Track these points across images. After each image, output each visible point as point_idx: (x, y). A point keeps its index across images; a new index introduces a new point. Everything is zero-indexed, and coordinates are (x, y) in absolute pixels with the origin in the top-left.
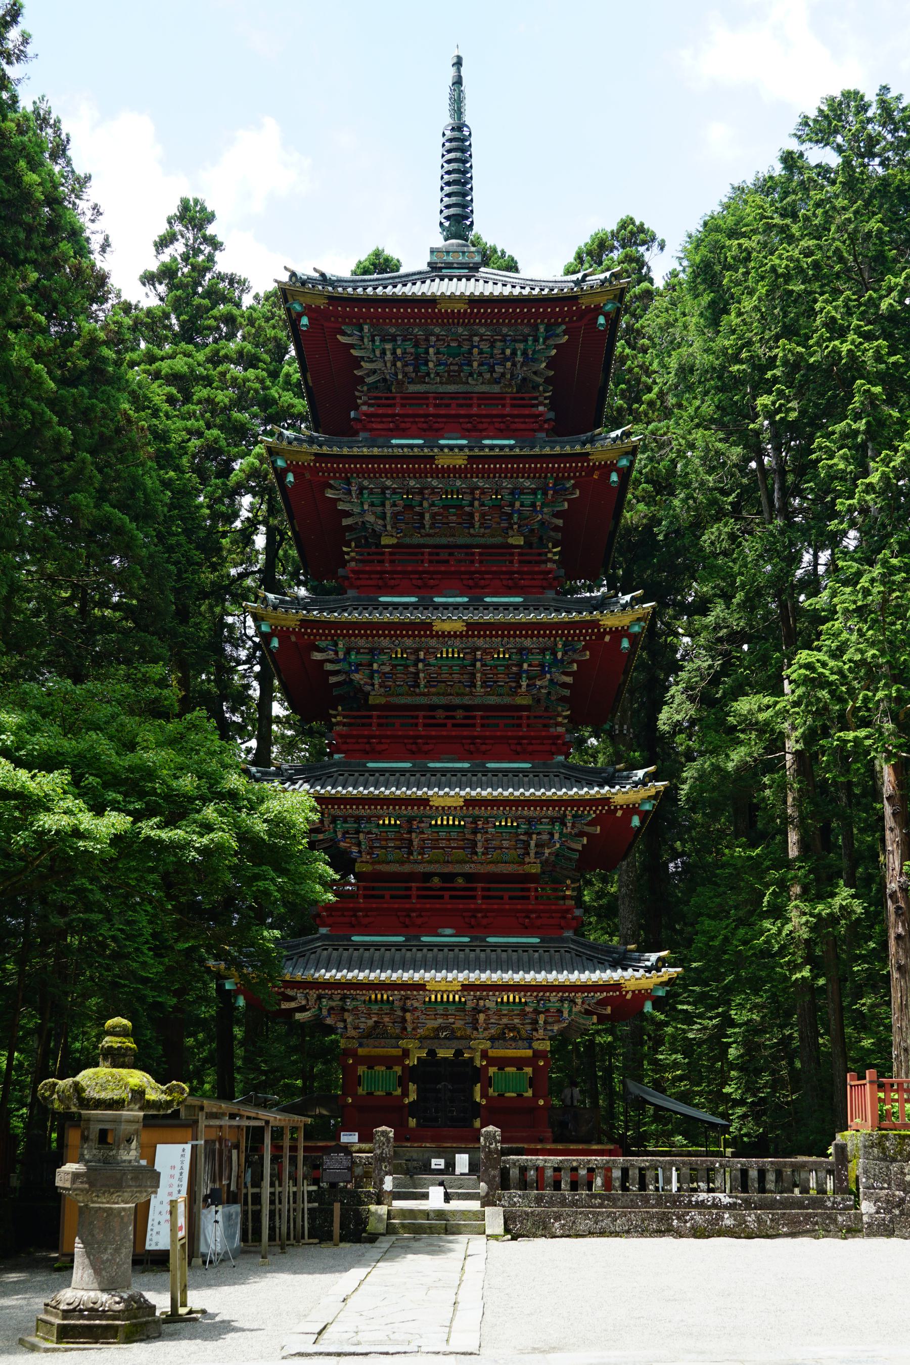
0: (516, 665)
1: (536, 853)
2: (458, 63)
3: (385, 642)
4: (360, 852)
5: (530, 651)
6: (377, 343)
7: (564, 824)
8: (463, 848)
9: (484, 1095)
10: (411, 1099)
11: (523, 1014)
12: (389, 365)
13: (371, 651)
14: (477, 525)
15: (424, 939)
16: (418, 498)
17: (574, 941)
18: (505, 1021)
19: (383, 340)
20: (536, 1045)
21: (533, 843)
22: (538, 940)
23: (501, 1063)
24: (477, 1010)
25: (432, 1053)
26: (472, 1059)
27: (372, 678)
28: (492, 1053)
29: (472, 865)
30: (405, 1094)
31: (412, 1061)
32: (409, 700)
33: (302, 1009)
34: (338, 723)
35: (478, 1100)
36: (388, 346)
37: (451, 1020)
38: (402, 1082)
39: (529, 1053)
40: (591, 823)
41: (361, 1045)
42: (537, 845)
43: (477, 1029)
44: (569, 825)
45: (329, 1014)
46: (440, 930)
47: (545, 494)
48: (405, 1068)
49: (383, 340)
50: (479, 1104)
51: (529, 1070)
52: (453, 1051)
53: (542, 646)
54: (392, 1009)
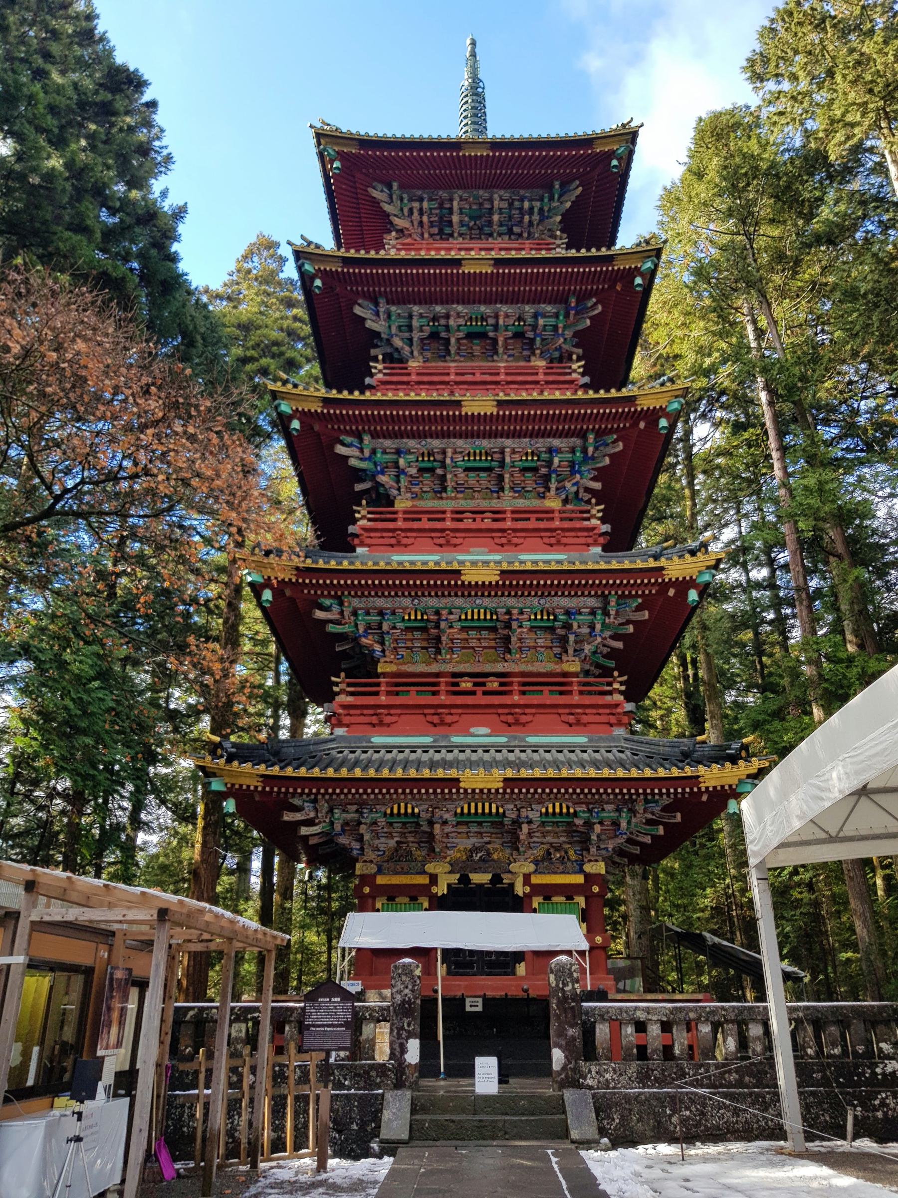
1: (575, 650)
2: (473, 43)
3: (412, 443)
4: (383, 651)
5: (559, 451)
6: (405, 201)
7: (606, 613)
8: (495, 648)
11: (570, 829)
12: (416, 223)
13: (398, 452)
14: (501, 350)
16: (443, 322)
17: (626, 739)
18: (549, 839)
19: (411, 200)
20: (588, 868)
21: (572, 638)
22: (586, 740)
24: (517, 823)
25: (464, 879)
26: (512, 885)
27: (398, 482)
28: (535, 880)
29: (505, 664)
33: (310, 823)
34: (363, 517)
36: (416, 205)
37: (487, 839)
39: (579, 879)
40: (639, 608)
41: (380, 871)
42: (576, 642)
43: (517, 849)
44: (612, 613)
45: (343, 830)
46: (473, 730)
47: (567, 316)
49: (411, 200)
52: (490, 876)
53: (571, 445)
54: (418, 824)
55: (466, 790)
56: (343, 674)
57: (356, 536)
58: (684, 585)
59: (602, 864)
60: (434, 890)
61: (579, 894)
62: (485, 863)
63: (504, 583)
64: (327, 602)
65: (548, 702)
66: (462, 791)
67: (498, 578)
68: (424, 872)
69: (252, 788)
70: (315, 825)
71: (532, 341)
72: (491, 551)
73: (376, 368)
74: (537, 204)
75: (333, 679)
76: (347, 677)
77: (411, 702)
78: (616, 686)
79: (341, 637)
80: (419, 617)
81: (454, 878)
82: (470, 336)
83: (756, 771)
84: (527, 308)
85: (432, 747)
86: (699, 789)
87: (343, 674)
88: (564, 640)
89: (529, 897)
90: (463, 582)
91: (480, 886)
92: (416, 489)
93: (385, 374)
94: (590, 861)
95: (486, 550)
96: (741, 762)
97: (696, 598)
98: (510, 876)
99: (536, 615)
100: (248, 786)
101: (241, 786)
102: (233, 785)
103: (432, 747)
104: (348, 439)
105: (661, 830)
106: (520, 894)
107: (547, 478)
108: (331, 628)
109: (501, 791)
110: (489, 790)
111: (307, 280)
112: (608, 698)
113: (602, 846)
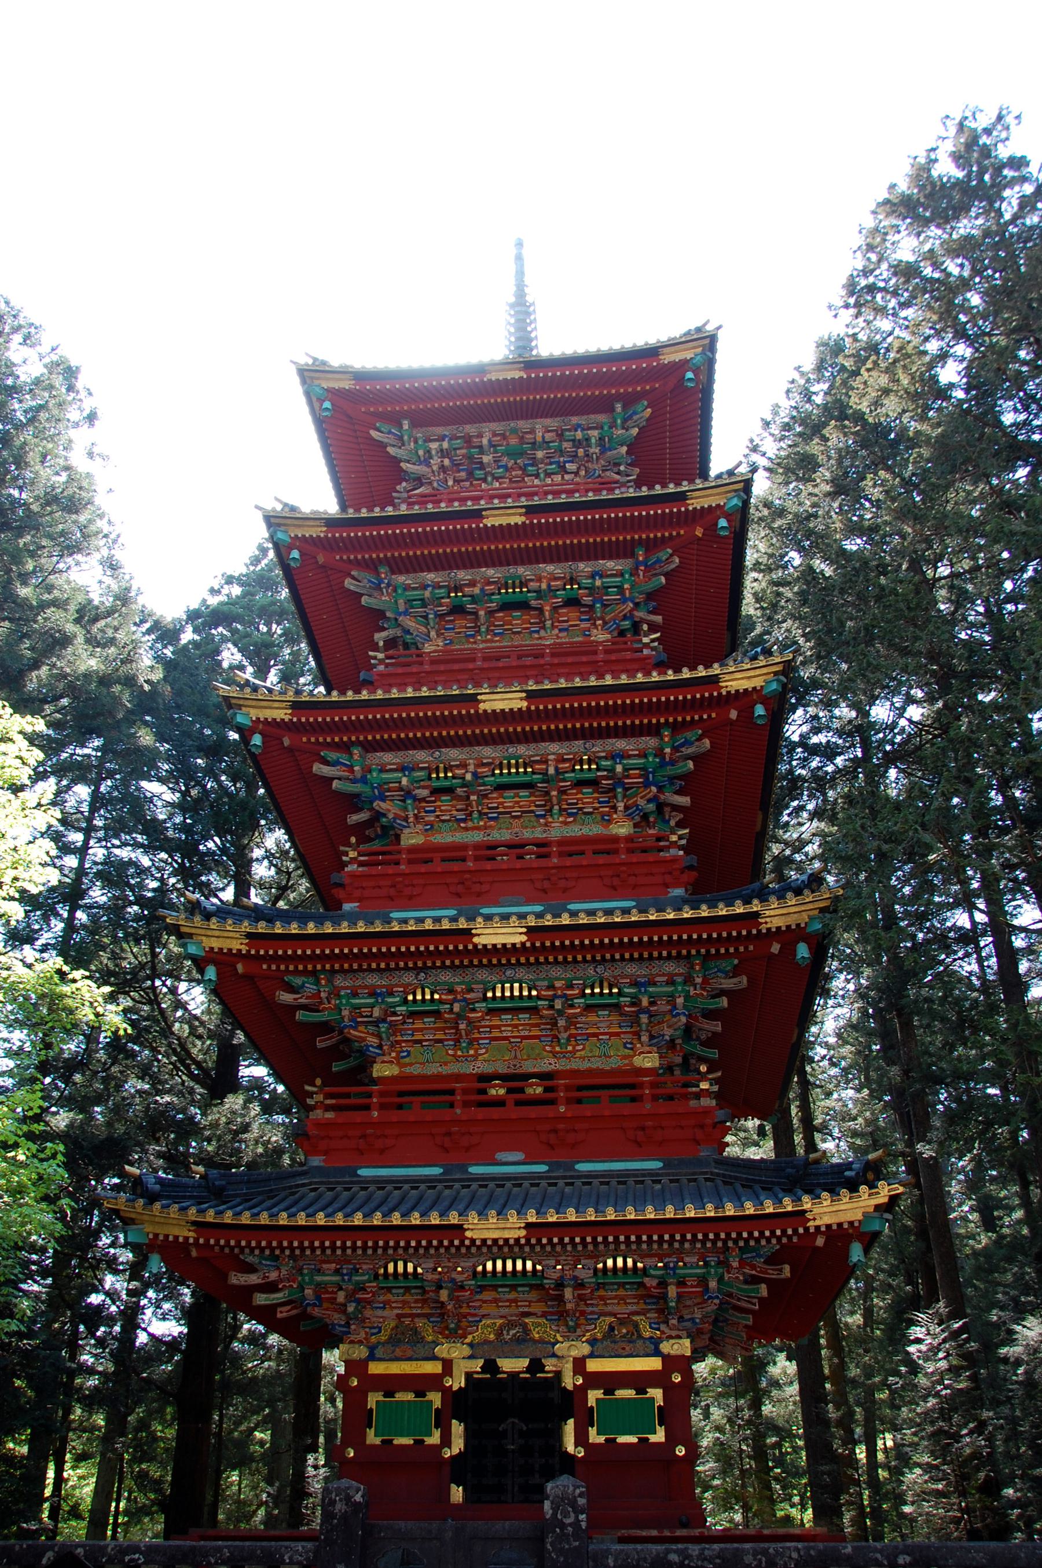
0: (606, 778)
1: (652, 1037)
4: (380, 1047)
5: (624, 755)
9: (581, 1439)
10: (455, 1451)
11: (645, 1294)
15: (474, 1170)
20: (666, 1347)
22: (660, 1164)
23: (610, 1381)
24: (560, 1285)
25: (490, 1366)
26: (558, 1374)
27: (405, 809)
28: (594, 1366)
29: (552, 1061)
30: (446, 1441)
31: (457, 1382)
32: (460, 837)
33: (270, 1287)
34: (353, 860)
35: (570, 1448)
36: (434, 446)
38: (442, 1421)
39: (654, 1364)
41: (372, 1357)
46: (501, 1156)
48: (446, 1391)
50: (573, 1457)
51: (656, 1394)
52: (525, 1363)
55: (473, 1241)
56: (318, 1081)
57: (341, 885)
58: (790, 936)
59: (687, 1342)
60: (448, 1382)
61: (655, 1386)
62: (522, 1342)
63: (533, 944)
64: (297, 981)
65: (607, 1113)
66: (467, 1242)
67: (524, 938)
68: (435, 1358)
69: (181, 1239)
70: (278, 1290)
71: (592, 607)
72: (529, 901)
73: (375, 658)
74: (595, 434)
75: (308, 1088)
76: (324, 1084)
77: (412, 1119)
78: (704, 1085)
79: (325, 1028)
80: (428, 997)
81: (477, 1365)
82: (507, 607)
83: (886, 1200)
84: (581, 565)
85: (440, 1181)
86: (807, 1229)
87: (318, 1081)
88: (635, 1020)
89: (581, 1391)
90: (475, 946)
91: (514, 1375)
92: (431, 818)
93: (387, 665)
94: (670, 1337)
95: (523, 899)
96: (863, 1188)
97: (806, 955)
98: (553, 1360)
99: (592, 988)
100: (176, 1237)
101: (167, 1236)
102: (156, 1235)
103: (440, 1181)
104: (332, 756)
105: (763, 1290)
106: (570, 1387)
107: (612, 790)
108: (300, 1016)
109: (523, 1241)
110: (506, 1240)
111: (283, 550)
112: (693, 1103)
113: (686, 1317)
